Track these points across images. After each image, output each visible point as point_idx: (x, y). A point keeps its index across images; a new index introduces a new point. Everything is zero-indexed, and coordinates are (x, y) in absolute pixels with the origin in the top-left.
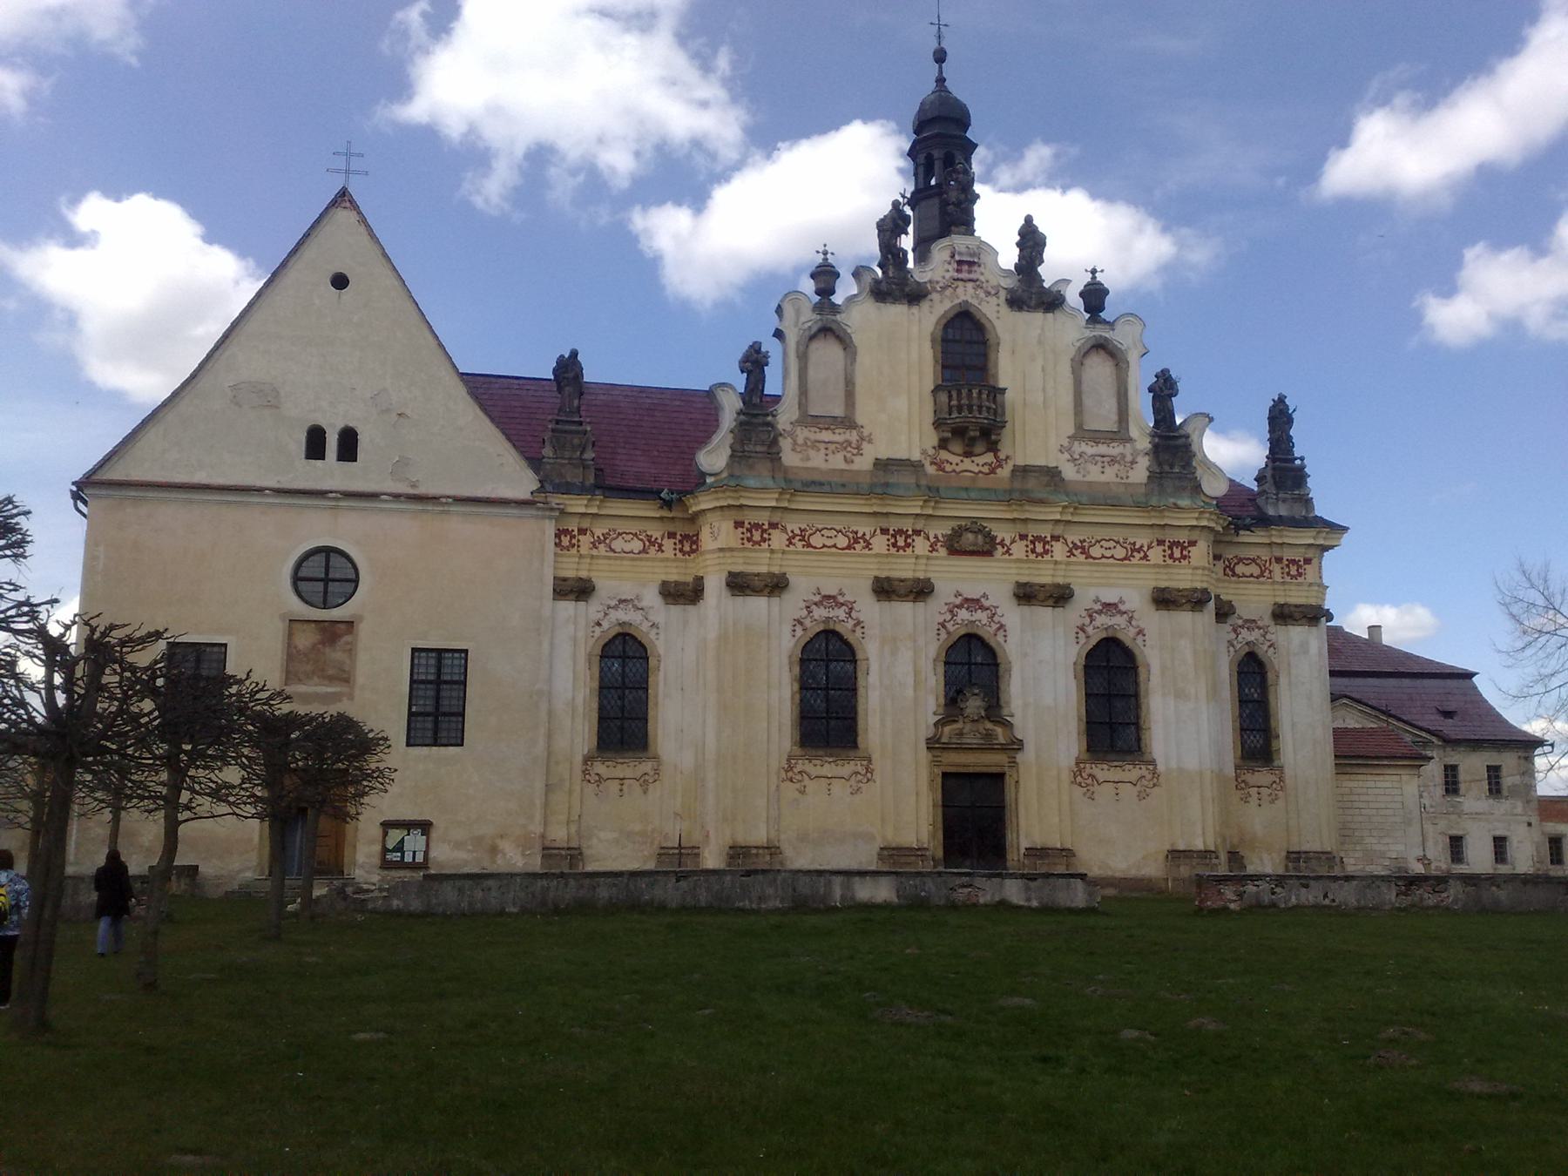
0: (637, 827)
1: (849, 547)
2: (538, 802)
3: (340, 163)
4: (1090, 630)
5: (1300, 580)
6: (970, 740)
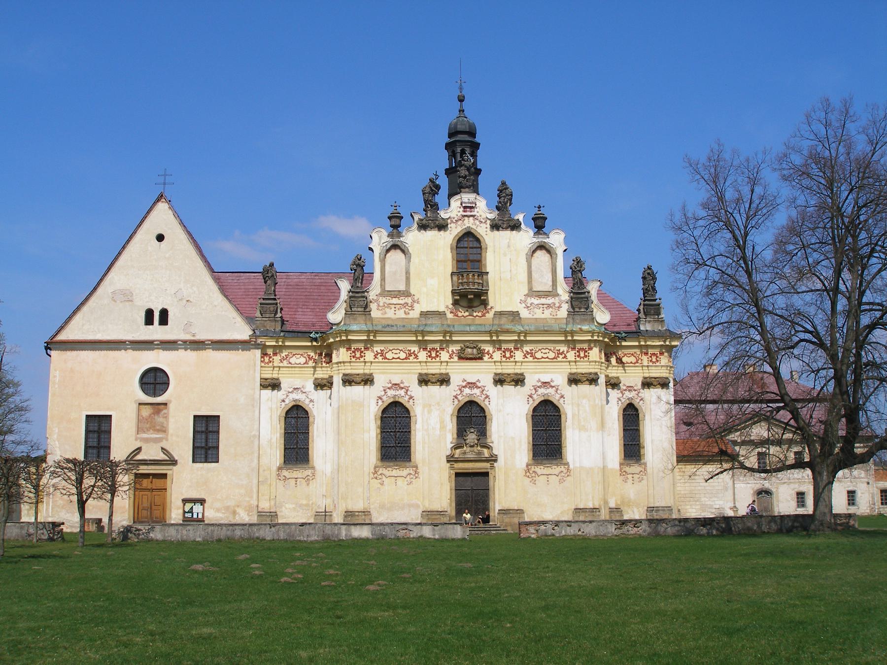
0: (304, 502)
1: (406, 358)
2: (255, 490)
3: (161, 180)
4: (535, 396)
5: (658, 364)
6: (470, 456)
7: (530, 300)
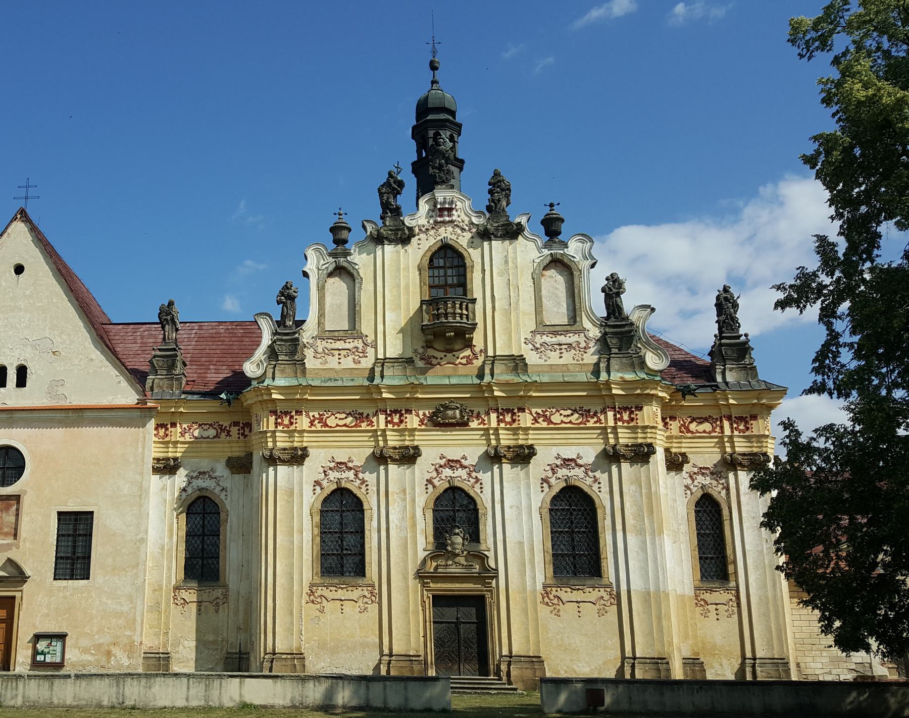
1: (356, 426)
7: (539, 339)
